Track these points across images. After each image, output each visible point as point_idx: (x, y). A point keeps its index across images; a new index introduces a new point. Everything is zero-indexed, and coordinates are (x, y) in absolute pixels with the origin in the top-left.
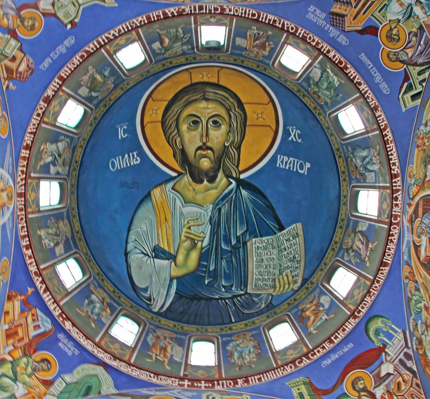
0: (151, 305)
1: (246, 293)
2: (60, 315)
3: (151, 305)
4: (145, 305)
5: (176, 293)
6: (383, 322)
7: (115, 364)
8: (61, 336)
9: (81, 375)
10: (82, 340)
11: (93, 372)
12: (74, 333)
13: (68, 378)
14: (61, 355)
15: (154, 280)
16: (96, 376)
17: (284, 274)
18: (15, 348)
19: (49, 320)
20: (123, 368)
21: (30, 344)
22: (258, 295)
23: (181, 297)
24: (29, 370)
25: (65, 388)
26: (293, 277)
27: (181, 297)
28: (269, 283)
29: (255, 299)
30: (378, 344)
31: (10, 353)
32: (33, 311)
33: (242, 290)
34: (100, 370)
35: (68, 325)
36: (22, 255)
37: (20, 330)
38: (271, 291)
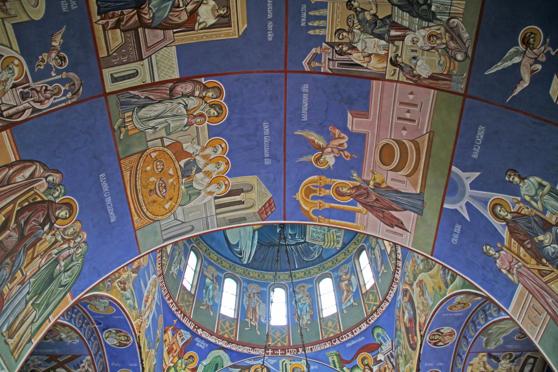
0: (242, 258)
1: (305, 242)
2: (194, 327)
3: (242, 258)
4: (238, 260)
5: (258, 242)
6: (382, 331)
7: (229, 346)
8: (197, 339)
9: (211, 358)
10: (208, 338)
11: (218, 354)
12: (205, 335)
13: (205, 363)
14: (198, 350)
15: (242, 234)
16: (219, 356)
17: (331, 231)
18: (174, 357)
19: (189, 333)
20: (234, 347)
21: (181, 351)
22: (313, 245)
23: (262, 245)
24: (184, 366)
25: (204, 369)
26: (337, 237)
27: (262, 245)
28: (321, 236)
29: (311, 248)
30: (377, 342)
31: (172, 362)
32: (179, 332)
33: (302, 239)
34: (221, 352)
35: (200, 331)
36: (168, 305)
37: (174, 346)
38: (322, 243)
